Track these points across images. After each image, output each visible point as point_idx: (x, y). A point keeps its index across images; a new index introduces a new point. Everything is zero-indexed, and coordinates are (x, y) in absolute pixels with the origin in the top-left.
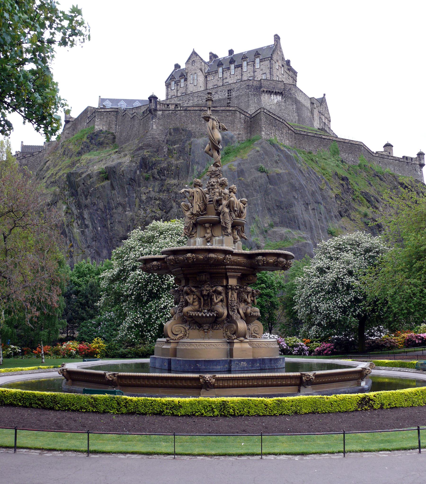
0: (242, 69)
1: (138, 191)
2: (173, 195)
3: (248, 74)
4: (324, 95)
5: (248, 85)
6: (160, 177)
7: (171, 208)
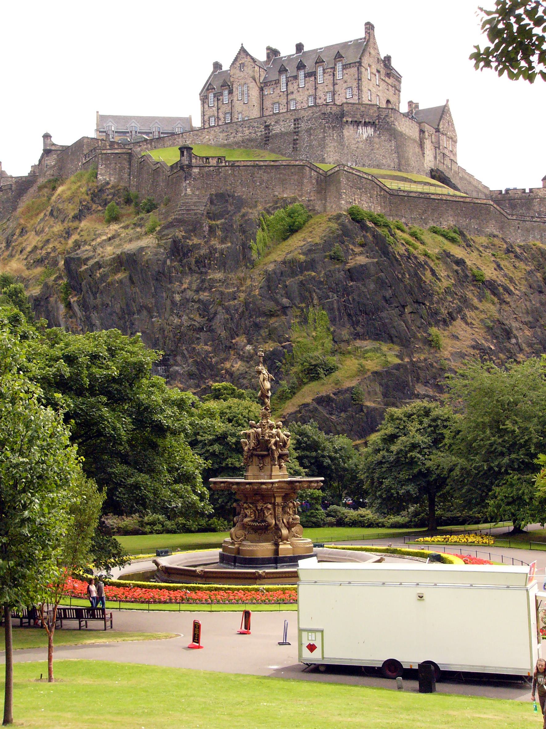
0: (315, 78)
1: (169, 289)
2: (217, 296)
3: (325, 88)
4: (448, 101)
5: (324, 114)
6: (199, 269)
7: (216, 314)
